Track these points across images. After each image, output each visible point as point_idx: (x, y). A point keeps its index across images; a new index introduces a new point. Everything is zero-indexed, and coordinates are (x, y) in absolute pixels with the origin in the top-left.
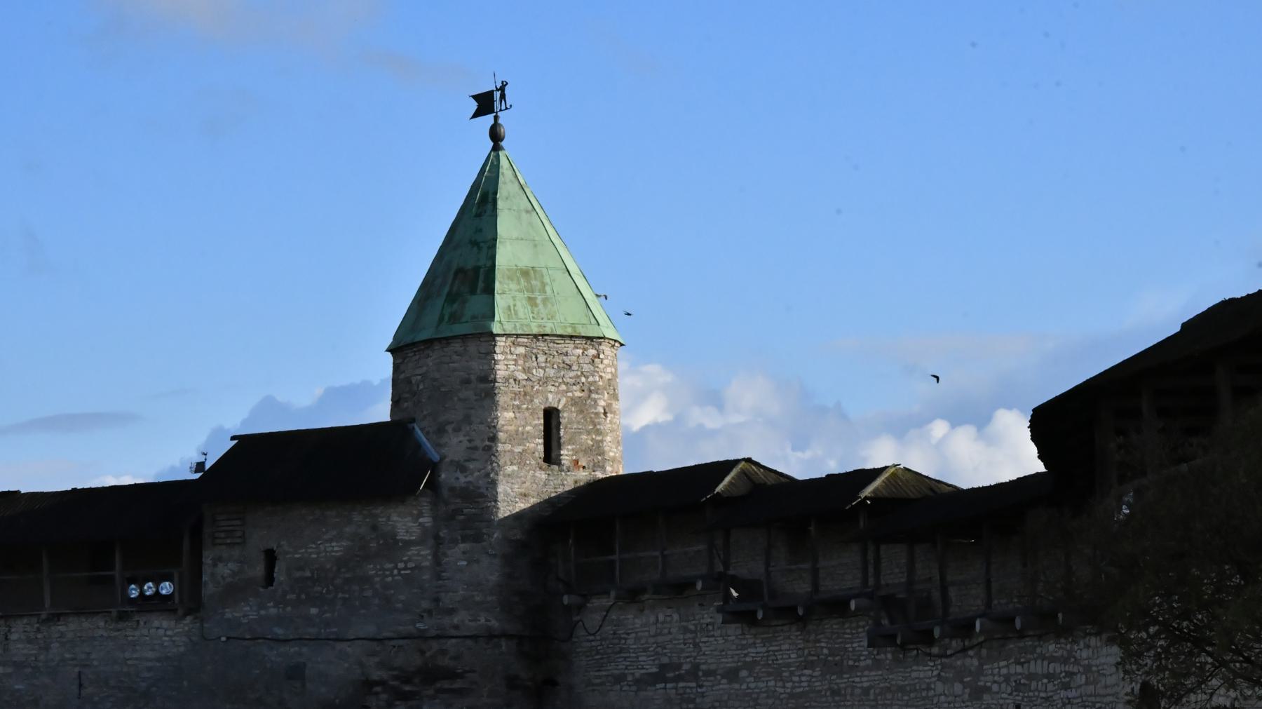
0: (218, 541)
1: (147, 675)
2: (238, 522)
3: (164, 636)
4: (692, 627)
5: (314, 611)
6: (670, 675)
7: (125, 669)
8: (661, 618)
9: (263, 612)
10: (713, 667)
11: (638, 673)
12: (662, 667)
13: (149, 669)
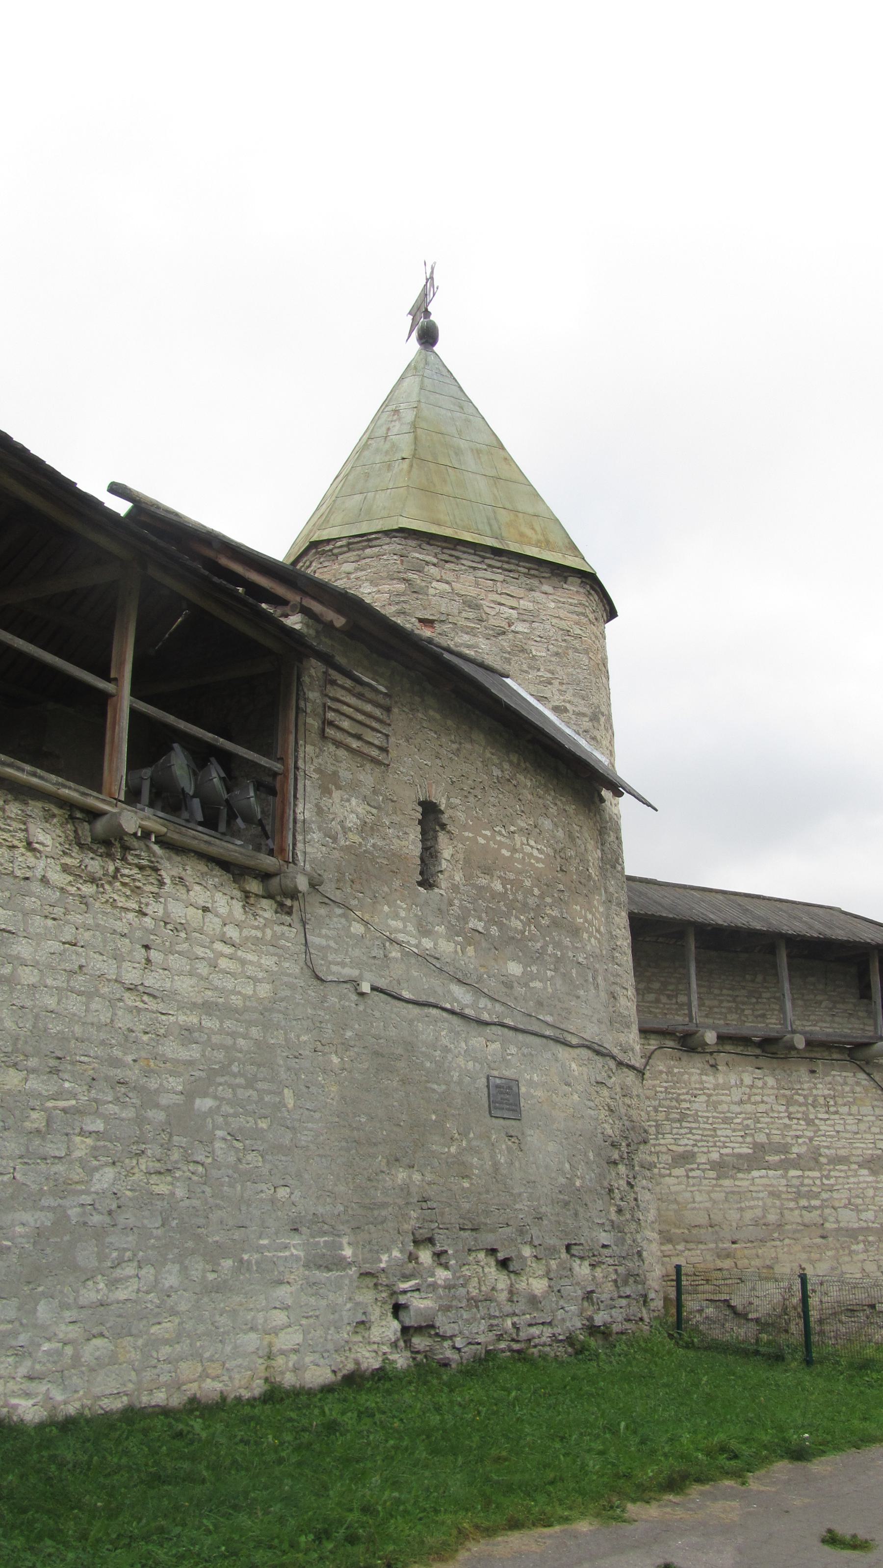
0: (330, 732)
1: (171, 1049)
2: (378, 712)
3: (202, 934)
4: (801, 1099)
5: (515, 969)
6: (773, 1158)
7: (124, 1021)
8: (747, 1080)
9: (427, 943)
10: (842, 1152)
11: (715, 1156)
12: (756, 1146)
13: (187, 1035)
